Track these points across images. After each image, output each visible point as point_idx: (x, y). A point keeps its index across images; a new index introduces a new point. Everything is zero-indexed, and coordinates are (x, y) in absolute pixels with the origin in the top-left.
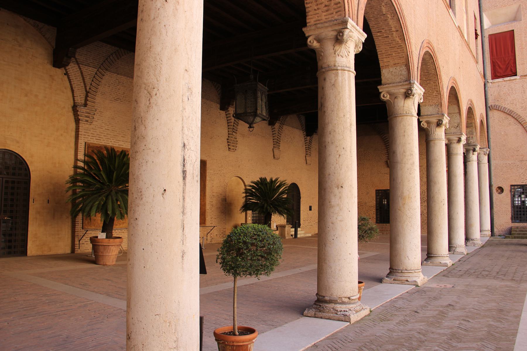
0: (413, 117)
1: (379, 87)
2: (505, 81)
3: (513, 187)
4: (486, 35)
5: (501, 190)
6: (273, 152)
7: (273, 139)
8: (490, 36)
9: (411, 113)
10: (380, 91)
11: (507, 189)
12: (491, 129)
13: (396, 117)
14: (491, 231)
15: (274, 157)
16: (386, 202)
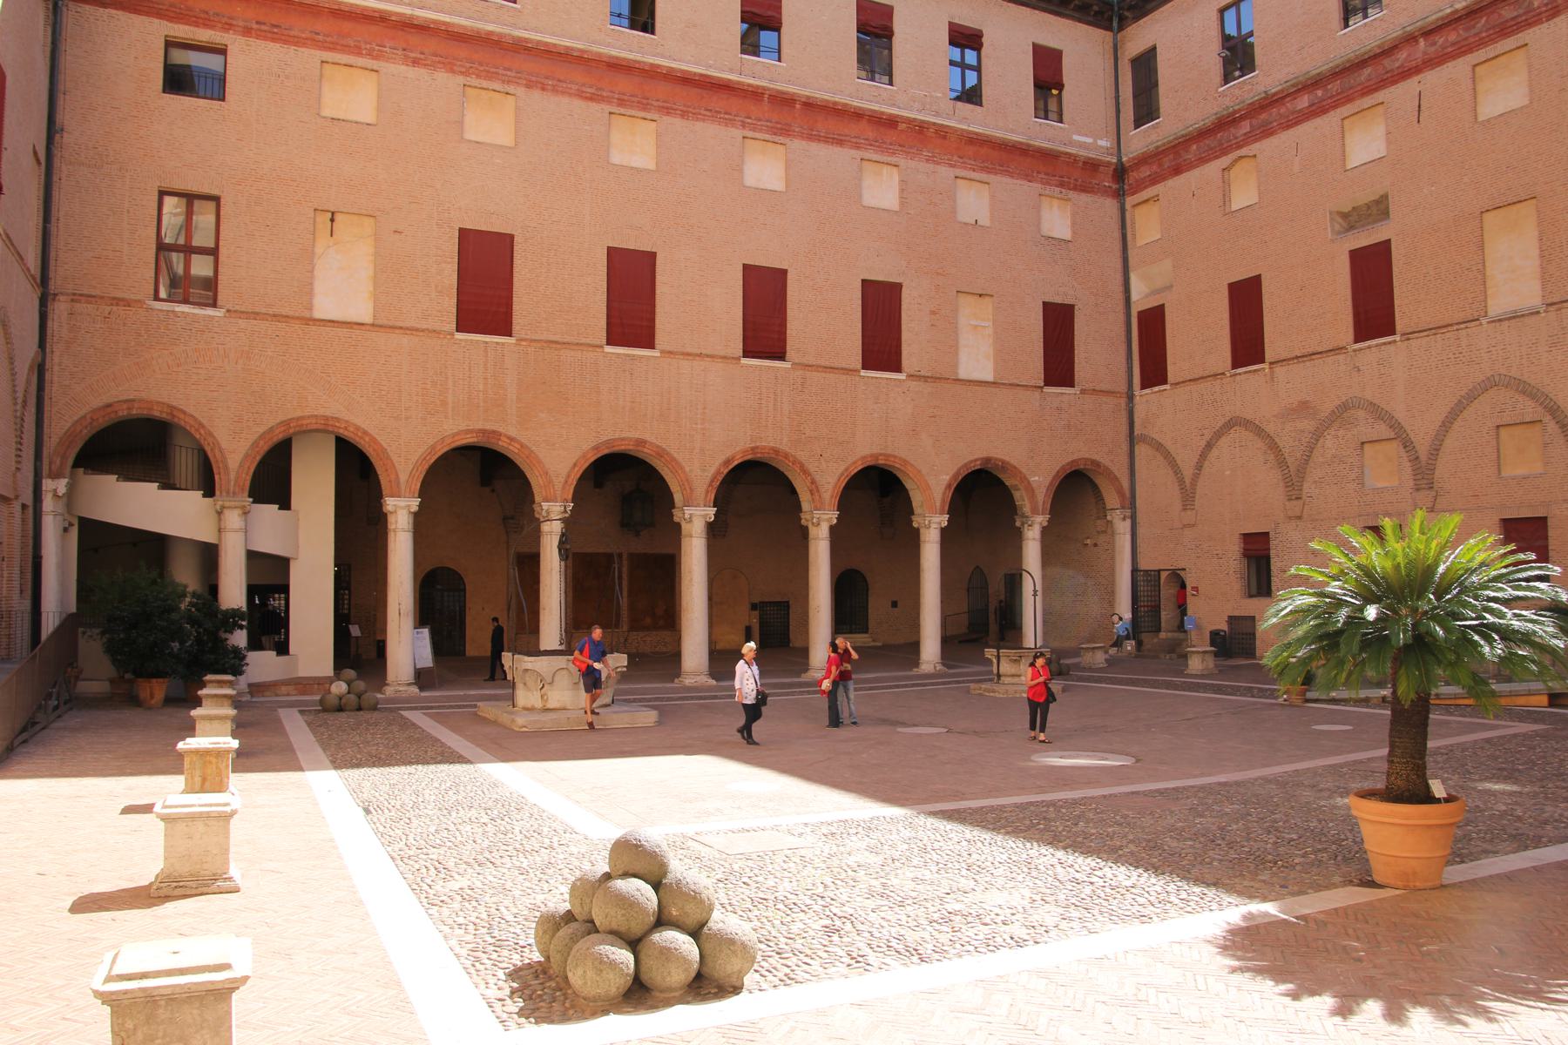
8: (1141, 314)
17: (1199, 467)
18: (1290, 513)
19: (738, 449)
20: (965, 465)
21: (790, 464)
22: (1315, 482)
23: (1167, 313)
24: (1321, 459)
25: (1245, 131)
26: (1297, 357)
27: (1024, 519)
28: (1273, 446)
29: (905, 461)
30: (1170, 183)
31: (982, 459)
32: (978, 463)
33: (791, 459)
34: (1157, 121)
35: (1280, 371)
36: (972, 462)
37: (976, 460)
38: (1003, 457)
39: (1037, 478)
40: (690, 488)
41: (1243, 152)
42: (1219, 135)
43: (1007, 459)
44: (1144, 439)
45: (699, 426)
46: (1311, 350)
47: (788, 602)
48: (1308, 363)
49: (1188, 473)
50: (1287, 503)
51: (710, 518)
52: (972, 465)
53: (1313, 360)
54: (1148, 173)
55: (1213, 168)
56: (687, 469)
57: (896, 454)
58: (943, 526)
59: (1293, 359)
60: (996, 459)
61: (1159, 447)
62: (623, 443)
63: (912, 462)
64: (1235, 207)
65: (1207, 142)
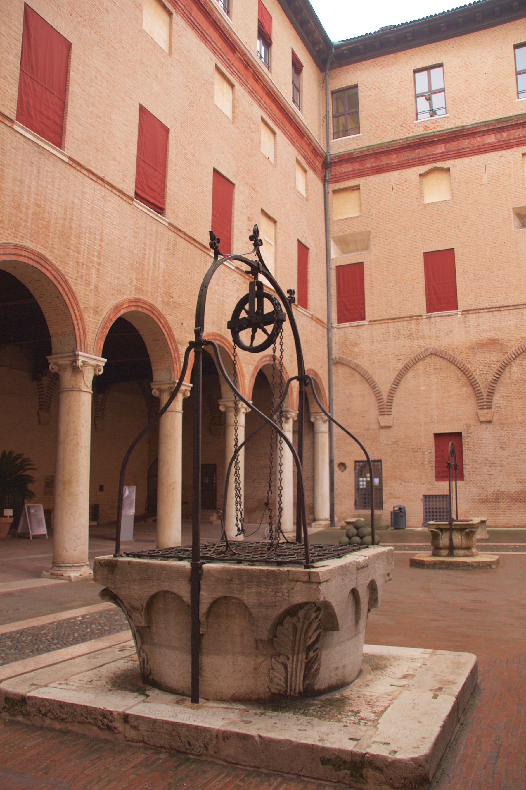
0: (81, 392)
1: (48, 357)
2: (352, 326)
3: (357, 464)
4: (333, 266)
5: (343, 466)
6: (39, 415)
7: (40, 399)
8: (338, 268)
9: (79, 388)
10: (49, 361)
11: (350, 466)
12: (334, 388)
13: (62, 392)
14: (330, 520)
15: (40, 422)
16: (207, 481)
17: (397, 383)
18: (482, 419)
19: (125, 297)
21: (161, 326)
22: (503, 396)
23: (365, 269)
24: (508, 381)
25: (440, 151)
26: (487, 308)
28: (464, 371)
30: (371, 178)
32: (268, 358)
33: (162, 321)
34: (358, 135)
35: (472, 317)
40: (84, 332)
41: (439, 165)
42: (417, 151)
44: (339, 362)
45: (95, 259)
46: (498, 304)
48: (495, 313)
49: (384, 388)
50: (478, 411)
51: (99, 371)
53: (500, 311)
54: (350, 169)
55: (413, 173)
56: (82, 307)
59: (483, 309)
61: (355, 369)
62: (24, 253)
64: (428, 200)
65: (406, 154)
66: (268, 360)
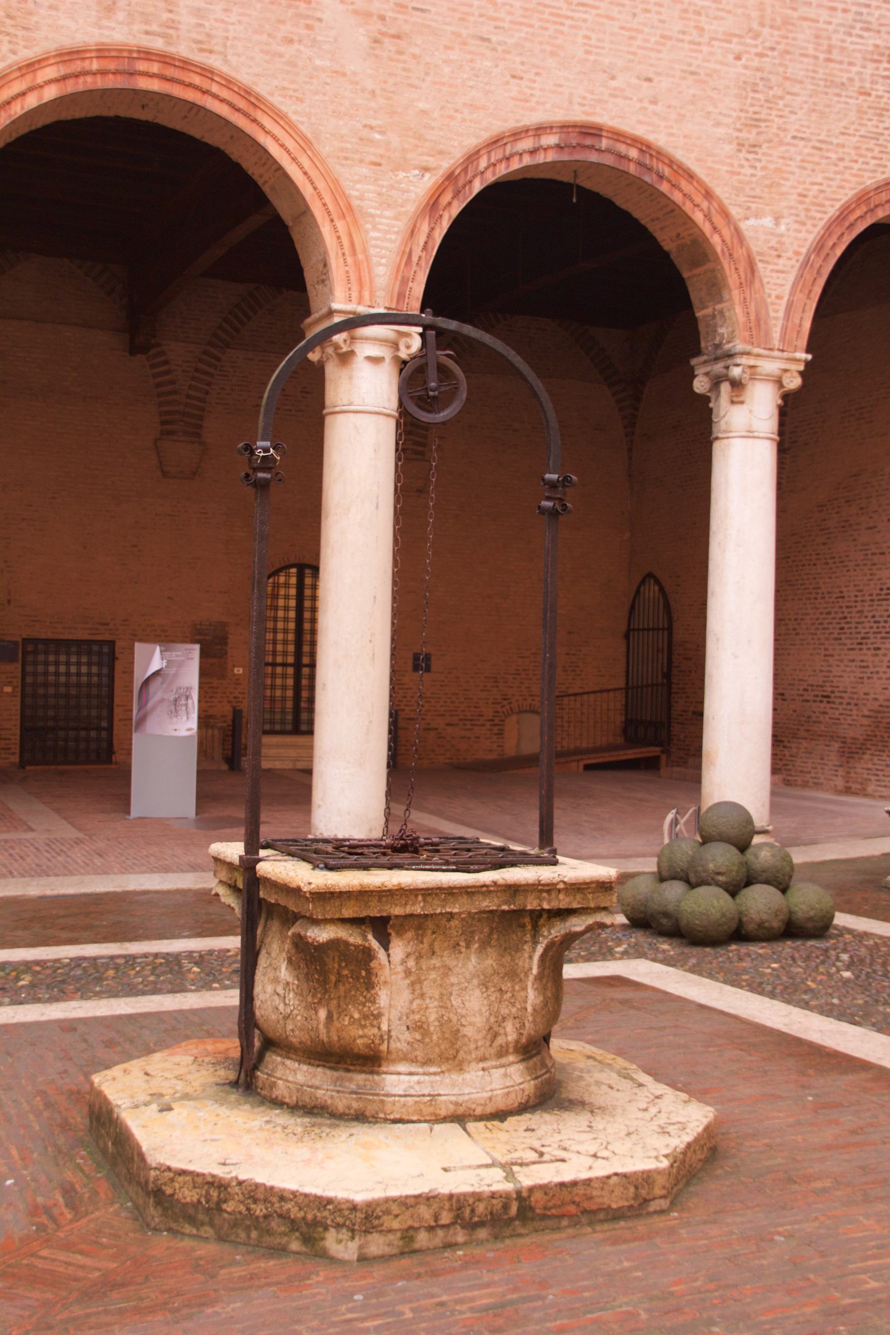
20: (496, 142)
27: (718, 368)
29: (246, 93)
31: (565, 127)
32: (550, 140)
36: (517, 135)
37: (540, 130)
38: (640, 131)
39: (767, 222)
43: (660, 139)
47: (112, 644)
52: (526, 144)
57: (214, 62)
58: (404, 354)
60: (618, 136)
63: (276, 100)
66: (558, 147)
